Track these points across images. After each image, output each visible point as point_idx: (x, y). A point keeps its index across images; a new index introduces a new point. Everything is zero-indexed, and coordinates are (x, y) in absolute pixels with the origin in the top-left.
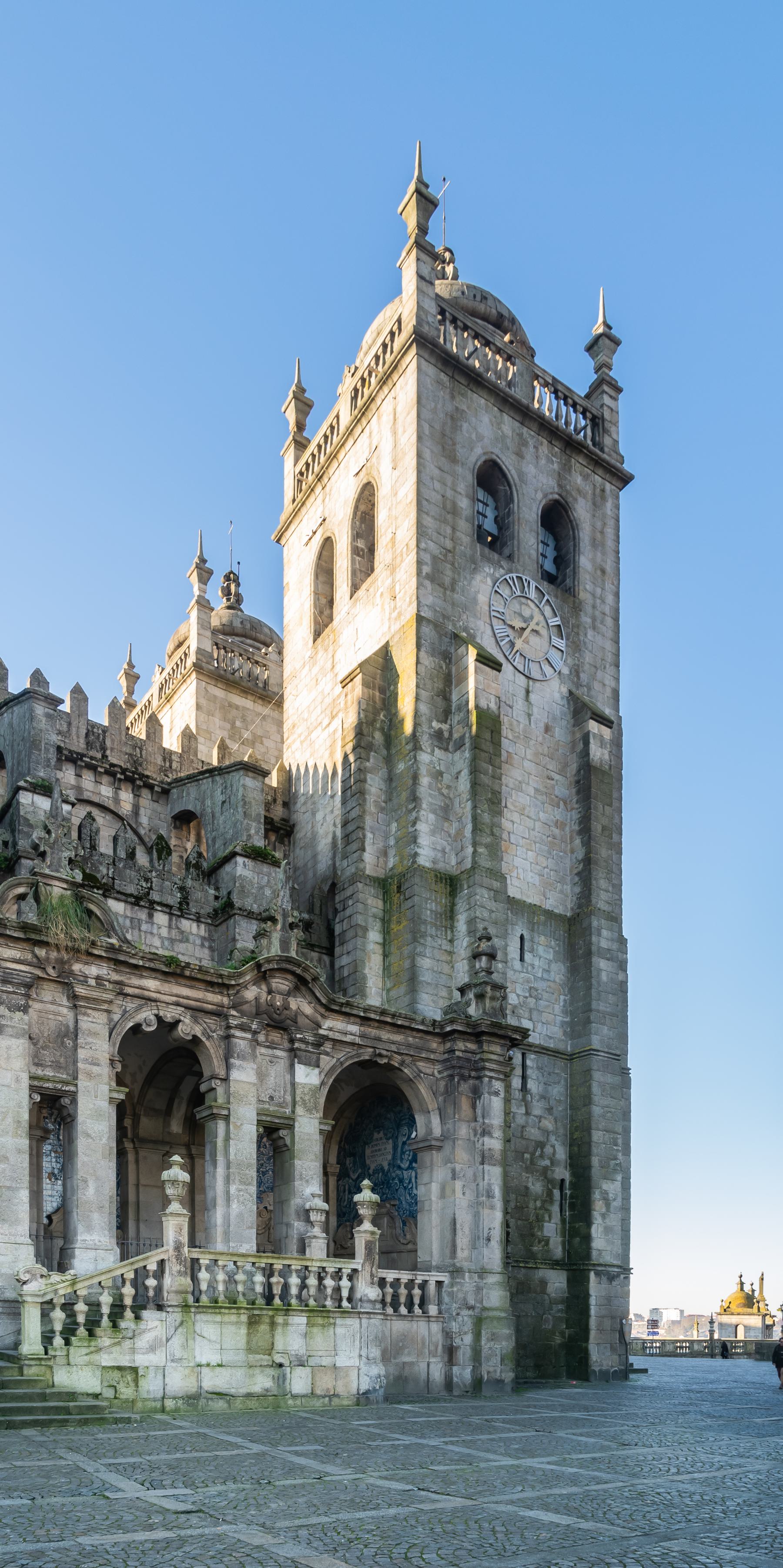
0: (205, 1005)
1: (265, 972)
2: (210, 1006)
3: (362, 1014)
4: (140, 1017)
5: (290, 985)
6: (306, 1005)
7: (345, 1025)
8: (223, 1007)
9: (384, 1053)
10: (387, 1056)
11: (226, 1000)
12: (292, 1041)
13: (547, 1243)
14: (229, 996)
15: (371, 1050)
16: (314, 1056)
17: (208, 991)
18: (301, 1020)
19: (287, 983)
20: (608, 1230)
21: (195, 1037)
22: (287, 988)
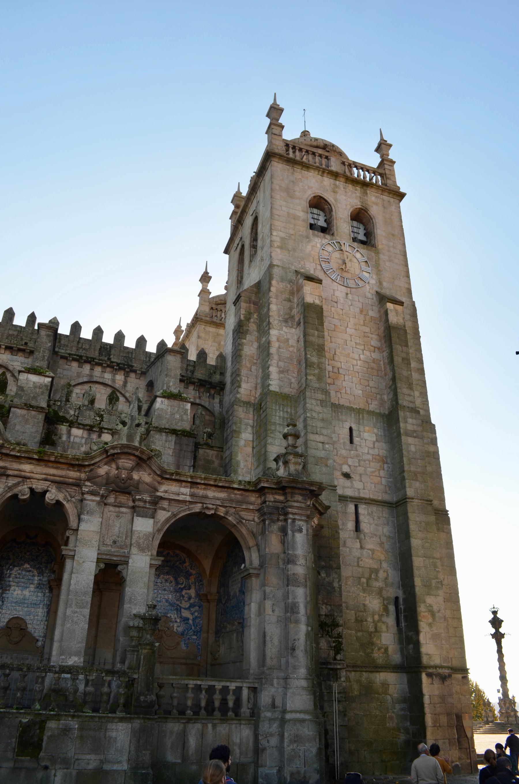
0: (67, 479)
1: (113, 455)
2: (71, 480)
3: (189, 480)
4: (16, 491)
5: (133, 463)
6: (146, 476)
7: (178, 488)
8: (81, 480)
9: (211, 506)
10: (213, 509)
11: (83, 476)
12: (134, 501)
13: (386, 649)
14: (85, 472)
15: (200, 505)
16: (150, 512)
17: (70, 470)
18: (141, 486)
19: (130, 462)
20: (436, 637)
21: (58, 502)
22: (131, 465)
